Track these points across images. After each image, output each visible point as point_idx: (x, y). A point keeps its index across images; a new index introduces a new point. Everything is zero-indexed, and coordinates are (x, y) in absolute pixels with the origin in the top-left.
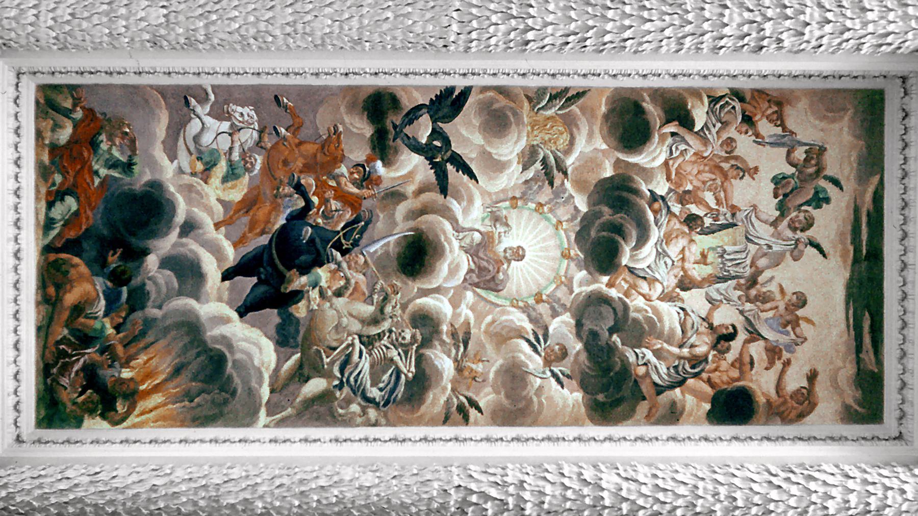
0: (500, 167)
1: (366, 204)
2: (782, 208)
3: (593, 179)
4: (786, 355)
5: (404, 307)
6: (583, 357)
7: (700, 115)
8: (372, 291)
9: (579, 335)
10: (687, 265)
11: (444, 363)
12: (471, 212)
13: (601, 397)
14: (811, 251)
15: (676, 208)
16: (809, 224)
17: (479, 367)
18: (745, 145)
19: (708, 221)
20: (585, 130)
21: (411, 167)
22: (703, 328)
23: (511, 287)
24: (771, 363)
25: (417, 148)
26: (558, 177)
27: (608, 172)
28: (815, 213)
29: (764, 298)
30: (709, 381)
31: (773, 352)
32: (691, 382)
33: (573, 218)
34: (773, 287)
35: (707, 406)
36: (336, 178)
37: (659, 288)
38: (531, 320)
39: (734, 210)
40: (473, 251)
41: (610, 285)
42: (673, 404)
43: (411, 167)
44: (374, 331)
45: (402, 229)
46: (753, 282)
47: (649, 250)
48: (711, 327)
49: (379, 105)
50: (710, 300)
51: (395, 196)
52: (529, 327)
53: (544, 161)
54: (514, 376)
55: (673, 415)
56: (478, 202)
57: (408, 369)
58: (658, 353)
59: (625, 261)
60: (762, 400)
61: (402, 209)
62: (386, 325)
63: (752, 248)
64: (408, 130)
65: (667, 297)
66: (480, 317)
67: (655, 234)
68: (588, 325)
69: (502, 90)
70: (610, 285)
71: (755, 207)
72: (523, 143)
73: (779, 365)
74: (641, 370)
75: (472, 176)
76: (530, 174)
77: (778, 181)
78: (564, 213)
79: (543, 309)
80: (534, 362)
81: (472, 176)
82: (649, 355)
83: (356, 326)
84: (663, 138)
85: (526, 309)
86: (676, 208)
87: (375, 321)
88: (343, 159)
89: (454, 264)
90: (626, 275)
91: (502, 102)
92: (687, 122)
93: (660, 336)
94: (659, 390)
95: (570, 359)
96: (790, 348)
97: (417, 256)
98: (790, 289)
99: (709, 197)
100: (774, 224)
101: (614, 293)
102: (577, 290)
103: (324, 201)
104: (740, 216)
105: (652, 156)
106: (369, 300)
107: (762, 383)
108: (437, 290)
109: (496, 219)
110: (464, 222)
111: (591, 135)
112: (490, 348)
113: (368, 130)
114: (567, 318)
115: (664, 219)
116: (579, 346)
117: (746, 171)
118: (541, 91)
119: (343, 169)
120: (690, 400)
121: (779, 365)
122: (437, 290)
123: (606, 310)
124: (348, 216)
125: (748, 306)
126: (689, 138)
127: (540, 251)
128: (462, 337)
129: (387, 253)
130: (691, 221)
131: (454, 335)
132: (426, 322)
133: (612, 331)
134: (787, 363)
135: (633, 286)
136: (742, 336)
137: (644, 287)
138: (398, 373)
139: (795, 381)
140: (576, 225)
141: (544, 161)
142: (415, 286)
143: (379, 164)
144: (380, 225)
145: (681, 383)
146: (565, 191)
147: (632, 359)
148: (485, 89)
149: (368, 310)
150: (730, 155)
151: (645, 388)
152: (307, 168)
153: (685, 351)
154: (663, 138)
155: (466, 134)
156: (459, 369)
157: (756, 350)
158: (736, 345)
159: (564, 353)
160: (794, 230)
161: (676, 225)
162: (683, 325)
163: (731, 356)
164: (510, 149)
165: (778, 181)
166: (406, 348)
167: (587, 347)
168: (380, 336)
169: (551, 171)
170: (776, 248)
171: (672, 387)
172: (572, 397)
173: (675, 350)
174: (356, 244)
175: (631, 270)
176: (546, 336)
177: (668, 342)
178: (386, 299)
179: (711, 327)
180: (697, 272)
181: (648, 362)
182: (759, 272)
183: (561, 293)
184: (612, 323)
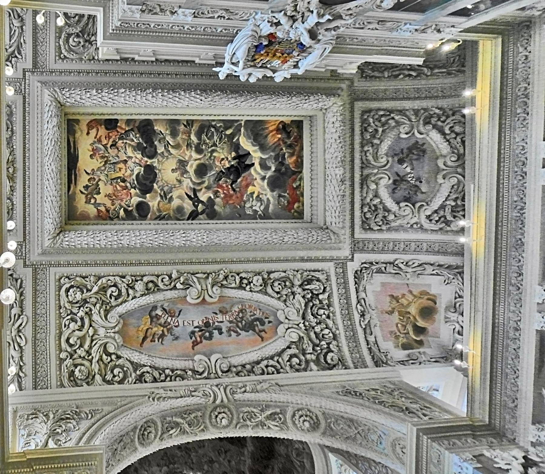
0: (180, 197)
1: (216, 185)
2: (98, 185)
3: (152, 193)
4: (96, 140)
5: (205, 155)
6: (154, 139)
7: (122, 212)
8: (214, 160)
9: (156, 146)
10: (124, 167)
11: (193, 138)
12: (187, 183)
13: (149, 127)
14: (89, 172)
15: (128, 185)
16: (89, 180)
17: (184, 137)
18: (108, 203)
19: (119, 181)
20: (155, 209)
21: (203, 196)
22: (120, 148)
23: (175, 161)
24: (100, 137)
25: (202, 202)
26: (162, 193)
27: (148, 195)
28: (88, 183)
29: (102, 157)
30: (118, 132)
31: (100, 141)
32: (123, 132)
33: (158, 181)
34: (100, 161)
35: (118, 125)
36: (224, 193)
37: (133, 160)
38: (169, 151)
39: (111, 184)
40: (187, 172)
41: (147, 161)
42: (128, 126)
43: (203, 196)
44: (213, 148)
45: (206, 179)
46: (106, 162)
47: (136, 173)
48: (118, 149)
49: (212, 215)
50: (118, 157)
51: (208, 188)
52: (170, 149)
53: (166, 198)
54: (174, 134)
55: (128, 122)
56: (185, 186)
57: (204, 136)
58: (133, 141)
59: (143, 169)
60: (103, 126)
61: (206, 184)
62: (210, 150)
63: (106, 172)
64: (205, 207)
65: (131, 158)
66: (184, 152)
67: (134, 177)
68: (153, 149)
69: (179, 220)
70: (147, 161)
71: (105, 185)
72: (173, 203)
73: (98, 137)
74: (138, 136)
75: (186, 194)
76: (170, 195)
77: (99, 193)
78: (160, 183)
79: (166, 154)
80: (168, 138)
81: (186, 194)
82: (135, 140)
83: (218, 149)
84: (132, 206)
85: (171, 154)
86: (128, 185)
87: (213, 151)
88: (222, 199)
89: (191, 168)
90: (142, 165)
91: (178, 216)
92: (125, 210)
93: (132, 146)
94: (132, 130)
95: (158, 139)
96: (95, 142)
97: (202, 170)
98: (95, 160)
99: (119, 188)
100: (100, 180)
101: (146, 159)
102: (156, 160)
103: (227, 186)
104: (110, 182)
105: (135, 200)
106: (215, 157)
107: (102, 131)
108: (196, 160)
109: (180, 181)
110: (189, 180)
111: (153, 206)
112: (181, 142)
113: (216, 207)
114: (159, 152)
115: (132, 181)
116: (156, 143)
117: (108, 196)
118: (168, 220)
119: (222, 196)
120: (123, 126)
121: (98, 137)
122: (196, 160)
123: (148, 154)
124: (221, 182)
125: (107, 155)
126: (125, 206)
127: (167, 171)
128: (189, 146)
129: (210, 171)
130: (124, 181)
131: (191, 147)
132: (199, 151)
133: (146, 148)
134: (95, 138)
135: (140, 161)
136: (109, 146)
137: (137, 161)
138: (206, 136)
139: (93, 132)
140: (157, 179)
141: (166, 198)
142: (202, 161)
143: (212, 197)
144: (212, 179)
145: (126, 132)
146: (161, 190)
147: (140, 139)
148: (183, 220)
149: (214, 154)
150: (113, 201)
151: (136, 130)
152: (231, 196)
153: (125, 141)
154: (132, 206)
155: (188, 206)
156: (189, 136)
157: (104, 142)
158: (110, 143)
159: (160, 141)
160: (94, 179)
161: (128, 180)
162: (126, 149)
163: (111, 140)
164: (176, 203)
165: (99, 193)
166: (205, 143)
167: (153, 143)
168: (212, 146)
169: (164, 196)
170: (99, 173)
171: (129, 130)
172: (158, 128)
173: (128, 142)
174: (218, 174)
175: (141, 166)
176: (165, 146)
177: (130, 145)
178: (210, 157)
179: (118, 149)
180: (121, 165)
181: (135, 138)
182: (104, 165)
183: (161, 159)
184: (147, 150)
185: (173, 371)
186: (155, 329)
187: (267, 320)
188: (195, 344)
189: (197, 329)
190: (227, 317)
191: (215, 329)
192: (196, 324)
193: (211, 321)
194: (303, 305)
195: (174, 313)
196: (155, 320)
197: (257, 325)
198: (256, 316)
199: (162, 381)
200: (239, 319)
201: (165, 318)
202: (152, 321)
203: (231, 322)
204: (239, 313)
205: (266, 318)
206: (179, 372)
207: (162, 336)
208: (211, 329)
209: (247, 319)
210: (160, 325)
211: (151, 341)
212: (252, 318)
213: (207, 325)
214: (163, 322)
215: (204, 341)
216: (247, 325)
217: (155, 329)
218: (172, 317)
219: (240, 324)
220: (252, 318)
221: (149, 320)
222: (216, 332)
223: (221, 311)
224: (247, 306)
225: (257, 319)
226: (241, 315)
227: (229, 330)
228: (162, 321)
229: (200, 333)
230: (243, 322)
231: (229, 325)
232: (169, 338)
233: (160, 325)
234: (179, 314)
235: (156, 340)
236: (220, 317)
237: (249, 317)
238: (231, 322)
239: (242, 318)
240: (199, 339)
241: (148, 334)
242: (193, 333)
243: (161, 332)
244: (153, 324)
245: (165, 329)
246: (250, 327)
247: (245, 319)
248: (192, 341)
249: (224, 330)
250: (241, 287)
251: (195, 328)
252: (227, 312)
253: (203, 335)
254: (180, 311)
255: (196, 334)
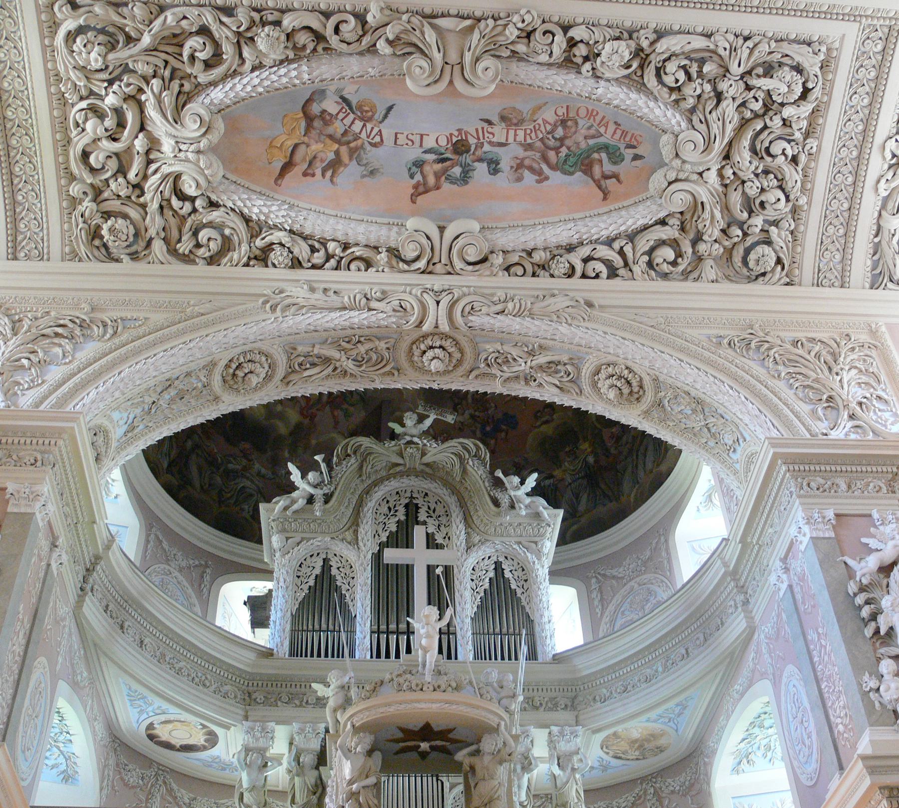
185: (346, 246)
186: (315, 147)
187: (631, 151)
188: (420, 190)
189: (431, 157)
190: (521, 133)
191: (480, 160)
192: (429, 143)
193: (472, 141)
194: (729, 128)
195: (373, 109)
196: (317, 123)
197: (601, 161)
198: (601, 140)
199: (314, 267)
200: (552, 143)
201: (347, 122)
202: (309, 127)
203: (528, 147)
204: (555, 126)
205: (630, 146)
206: (358, 251)
207: (335, 165)
208: (468, 158)
209: (578, 144)
210: (331, 137)
211: (305, 174)
212: (591, 142)
213: (460, 147)
214: (341, 130)
215: (446, 186)
216: (572, 160)
217: (315, 147)
218: (365, 120)
219: (552, 155)
220: (591, 142)
221: (303, 124)
222: (481, 169)
223: (503, 118)
224: (583, 113)
225: (605, 148)
226: (560, 132)
227: (520, 166)
228: (338, 128)
229: (438, 166)
230: (564, 151)
231: (521, 153)
232: (350, 172)
233: (331, 137)
234: (386, 116)
235: (318, 172)
236: (499, 133)
237: (580, 140)
238: (528, 147)
239: (562, 140)
240: (431, 180)
241: (298, 157)
242: (419, 164)
243: (331, 156)
244: (314, 133)
245: (344, 150)
246: (584, 163)
247: (568, 142)
248: (414, 181)
249: (505, 165)
250: (568, 63)
251: (425, 152)
252: (521, 122)
253: (445, 170)
254: (390, 108)
255: (427, 168)
